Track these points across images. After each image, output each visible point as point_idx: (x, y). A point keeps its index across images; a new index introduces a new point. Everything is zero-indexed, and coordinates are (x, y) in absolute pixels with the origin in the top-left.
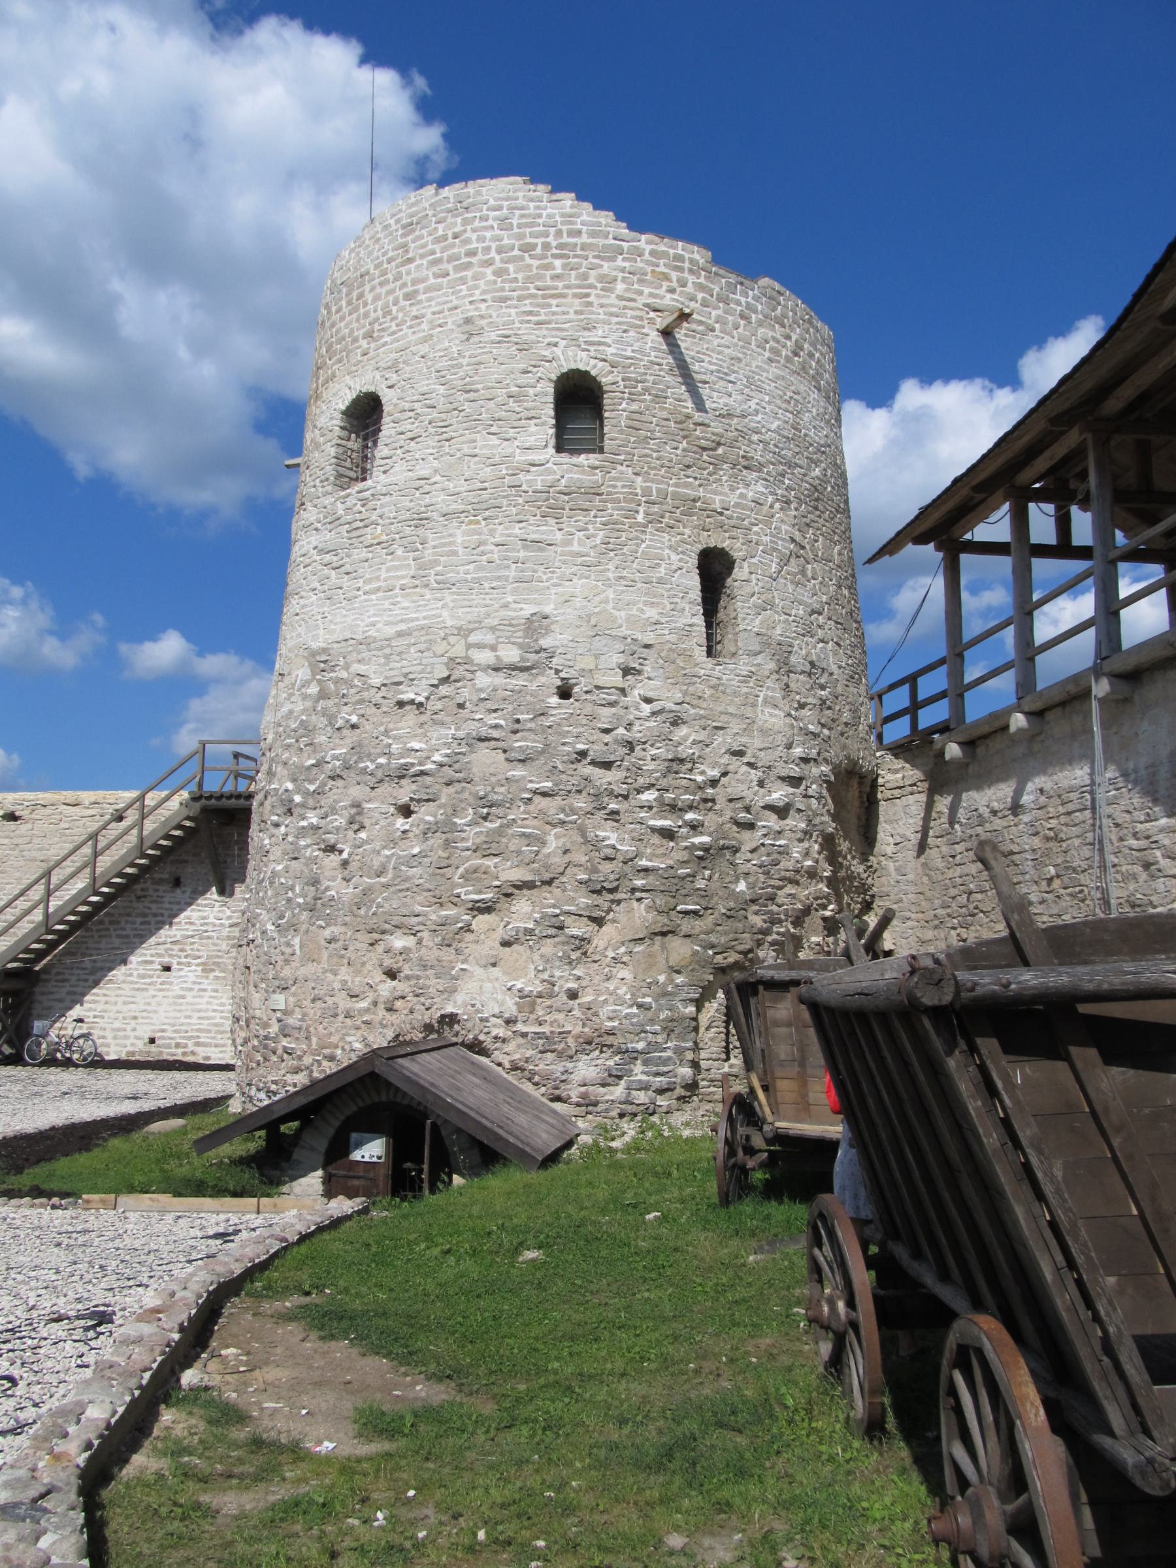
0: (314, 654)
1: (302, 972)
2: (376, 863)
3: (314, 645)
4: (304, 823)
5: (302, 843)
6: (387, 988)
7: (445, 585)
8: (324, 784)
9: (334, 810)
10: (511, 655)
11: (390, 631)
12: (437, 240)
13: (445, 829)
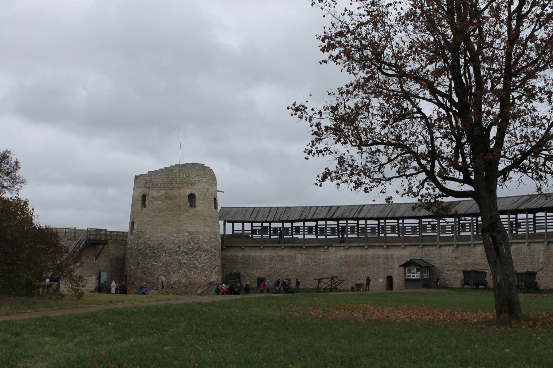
0: (189, 232)
1: (194, 276)
2: (204, 262)
3: (189, 230)
4: (191, 256)
5: (191, 259)
6: (206, 278)
7: (208, 226)
8: (194, 251)
9: (196, 255)
10: (215, 236)
11: (203, 231)
12: (202, 174)
13: (210, 258)
